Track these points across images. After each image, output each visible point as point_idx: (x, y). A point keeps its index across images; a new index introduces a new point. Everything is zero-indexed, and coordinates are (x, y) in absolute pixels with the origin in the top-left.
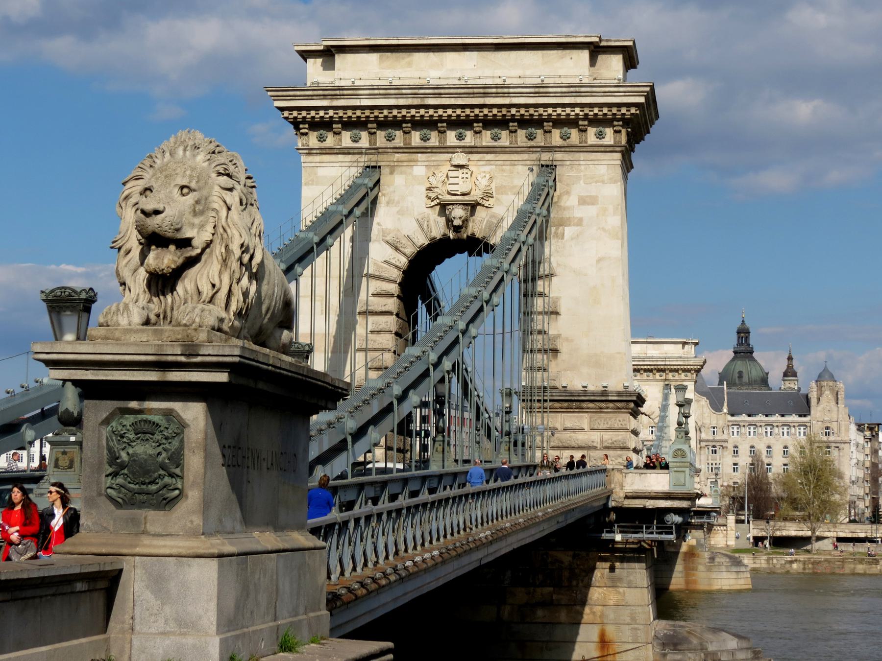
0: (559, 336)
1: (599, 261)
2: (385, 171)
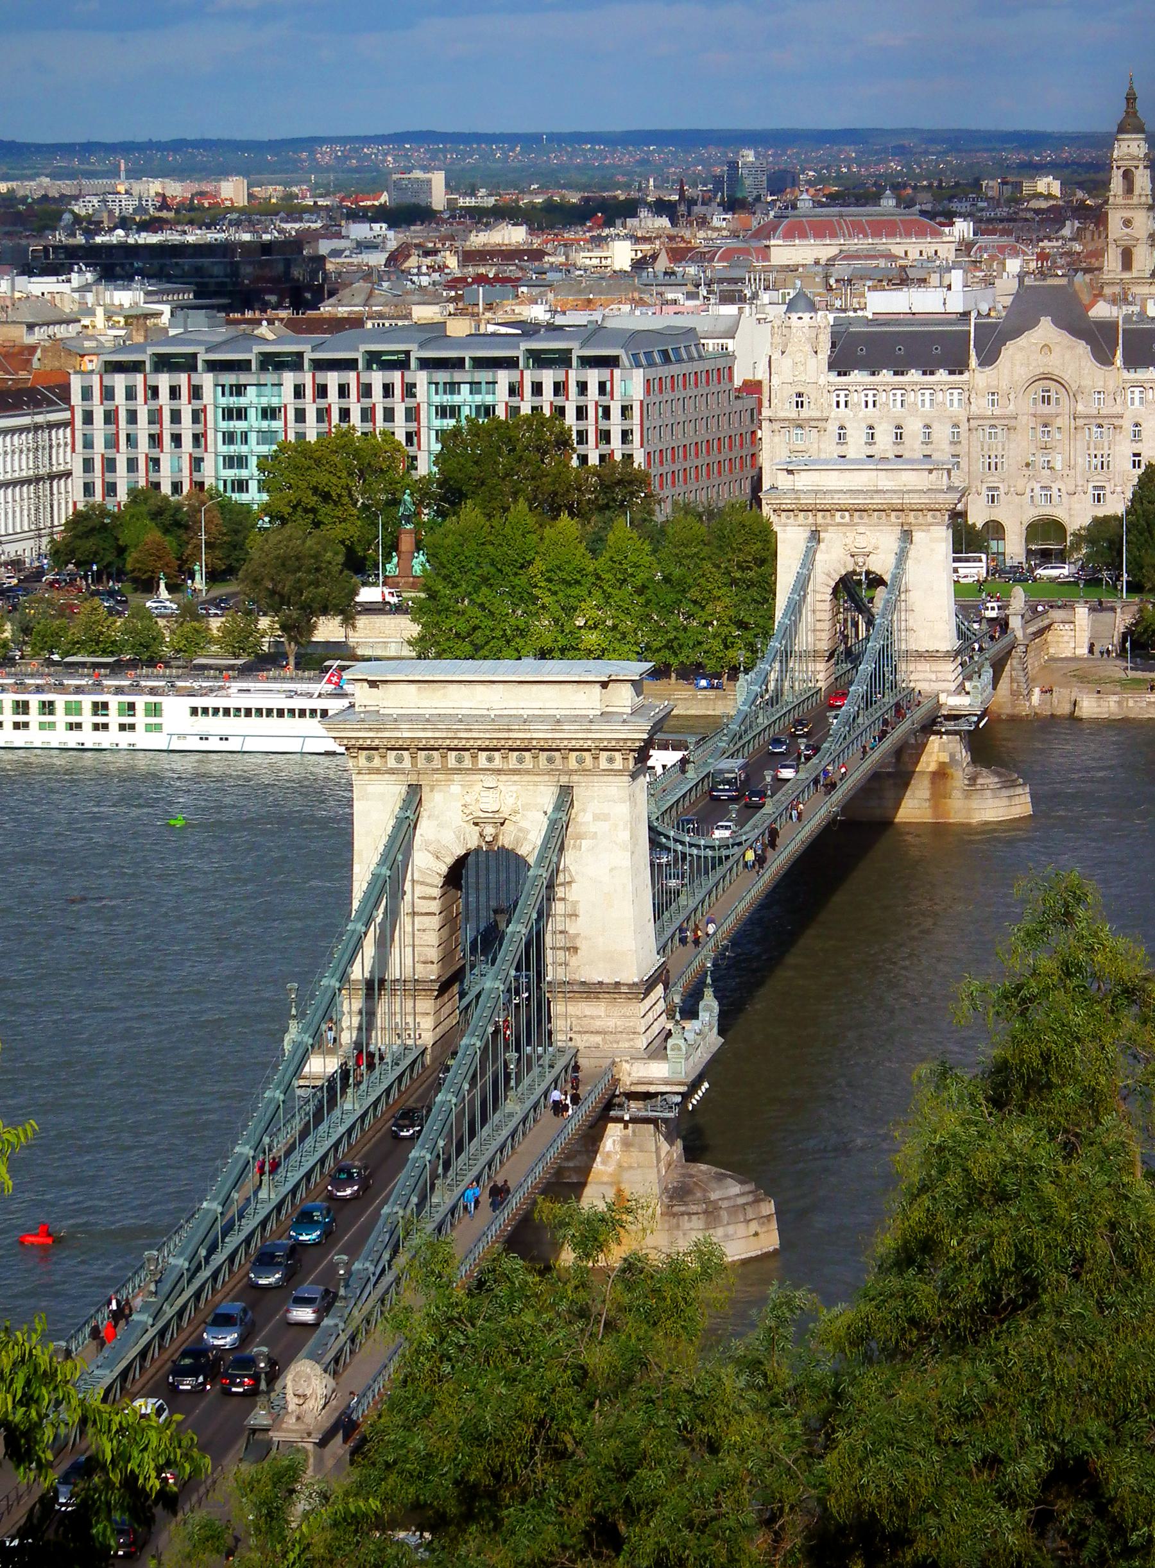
0: (578, 935)
1: (611, 870)
2: (425, 789)
